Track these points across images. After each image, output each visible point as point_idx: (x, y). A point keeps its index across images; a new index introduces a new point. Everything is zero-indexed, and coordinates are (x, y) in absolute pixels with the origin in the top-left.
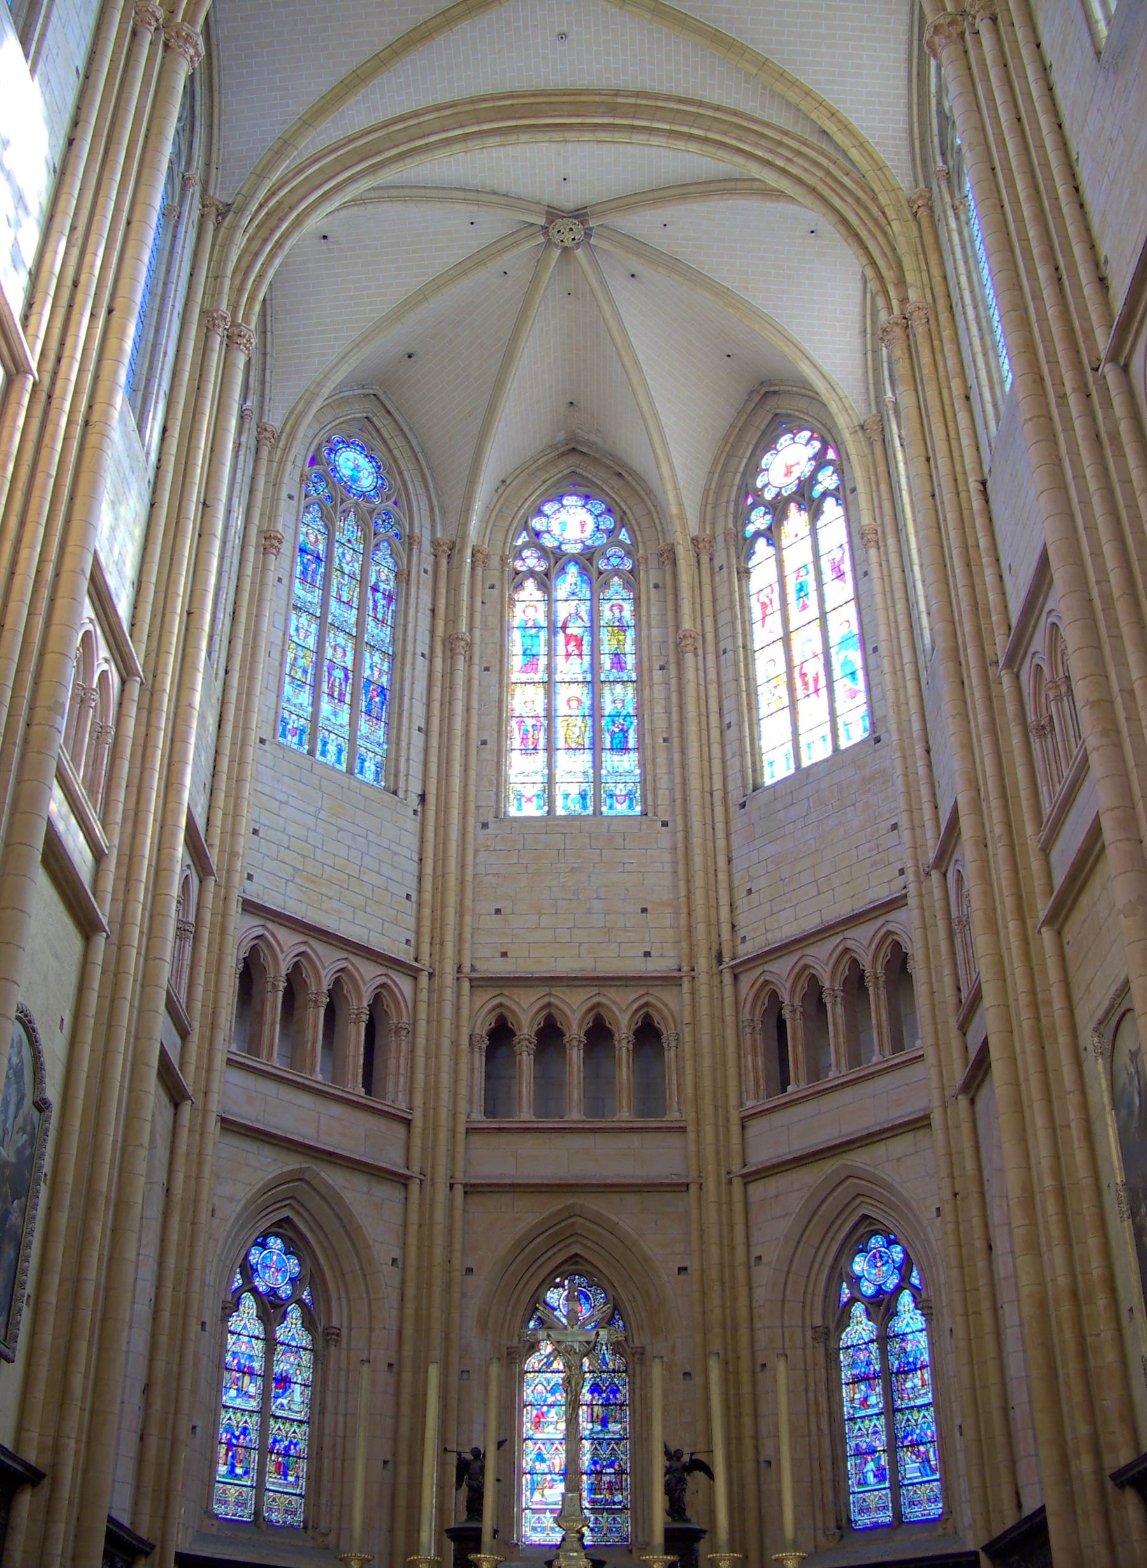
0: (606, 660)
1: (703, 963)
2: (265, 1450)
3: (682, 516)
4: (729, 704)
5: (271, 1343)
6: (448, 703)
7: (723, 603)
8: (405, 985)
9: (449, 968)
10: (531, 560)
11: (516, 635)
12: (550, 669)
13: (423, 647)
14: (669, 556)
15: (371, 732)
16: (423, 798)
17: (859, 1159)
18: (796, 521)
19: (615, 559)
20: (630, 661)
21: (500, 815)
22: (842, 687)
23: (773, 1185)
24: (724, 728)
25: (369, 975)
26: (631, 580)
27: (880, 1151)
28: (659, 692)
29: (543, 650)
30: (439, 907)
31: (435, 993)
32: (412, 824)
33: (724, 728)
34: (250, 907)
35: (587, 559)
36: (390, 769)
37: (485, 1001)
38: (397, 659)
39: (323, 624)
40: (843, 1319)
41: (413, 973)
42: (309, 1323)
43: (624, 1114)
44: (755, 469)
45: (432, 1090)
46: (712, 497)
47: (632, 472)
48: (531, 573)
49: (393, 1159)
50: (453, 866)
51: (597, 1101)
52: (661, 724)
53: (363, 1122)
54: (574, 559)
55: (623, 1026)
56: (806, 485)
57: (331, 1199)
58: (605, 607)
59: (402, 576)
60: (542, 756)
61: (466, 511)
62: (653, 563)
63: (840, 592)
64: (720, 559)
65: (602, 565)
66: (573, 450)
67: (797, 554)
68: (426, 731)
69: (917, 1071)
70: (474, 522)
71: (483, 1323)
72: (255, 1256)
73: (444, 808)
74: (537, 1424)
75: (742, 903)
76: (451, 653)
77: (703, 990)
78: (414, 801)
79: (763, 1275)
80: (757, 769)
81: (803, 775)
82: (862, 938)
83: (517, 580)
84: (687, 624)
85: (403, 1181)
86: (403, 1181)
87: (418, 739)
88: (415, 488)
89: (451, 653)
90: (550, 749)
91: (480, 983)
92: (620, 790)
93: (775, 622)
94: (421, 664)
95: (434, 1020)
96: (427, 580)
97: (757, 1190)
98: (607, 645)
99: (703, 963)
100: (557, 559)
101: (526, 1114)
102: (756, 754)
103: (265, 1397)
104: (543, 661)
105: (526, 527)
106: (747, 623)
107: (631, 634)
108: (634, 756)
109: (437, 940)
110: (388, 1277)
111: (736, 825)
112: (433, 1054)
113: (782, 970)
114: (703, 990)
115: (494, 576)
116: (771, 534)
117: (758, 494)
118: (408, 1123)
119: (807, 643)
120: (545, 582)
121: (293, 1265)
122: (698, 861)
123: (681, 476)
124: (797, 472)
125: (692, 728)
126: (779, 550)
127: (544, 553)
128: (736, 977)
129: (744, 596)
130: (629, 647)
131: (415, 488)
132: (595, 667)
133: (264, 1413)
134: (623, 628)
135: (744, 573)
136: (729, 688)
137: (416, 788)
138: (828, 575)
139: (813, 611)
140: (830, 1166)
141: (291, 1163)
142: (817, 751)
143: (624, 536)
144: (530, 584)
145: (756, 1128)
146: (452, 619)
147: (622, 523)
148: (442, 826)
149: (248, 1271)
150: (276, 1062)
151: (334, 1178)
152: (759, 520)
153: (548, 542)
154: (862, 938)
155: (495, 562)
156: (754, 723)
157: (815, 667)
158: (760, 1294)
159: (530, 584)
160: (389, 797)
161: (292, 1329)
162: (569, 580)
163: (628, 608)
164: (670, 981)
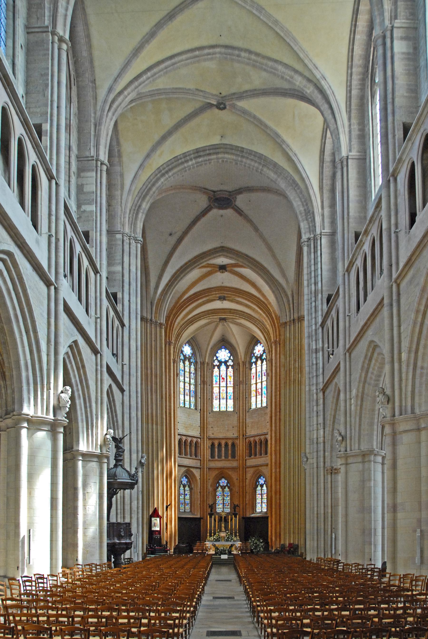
0: (228, 383)
1: (241, 437)
2: (185, 503)
3: (241, 358)
4: (247, 394)
5: (185, 490)
6: (204, 393)
7: (247, 375)
8: (199, 440)
9: (205, 437)
10: (216, 363)
11: (214, 377)
12: (220, 384)
13: (199, 383)
14: (239, 364)
15: (193, 400)
16: (201, 410)
17: (260, 468)
18: (259, 362)
19: (230, 363)
20: (232, 383)
21: (212, 411)
22: (263, 395)
23: (249, 469)
24: (246, 398)
25: (195, 440)
26: (233, 367)
27: (262, 467)
28: (236, 390)
29: (218, 381)
30: (204, 427)
31: (204, 441)
32: (199, 414)
33: (246, 398)
34: (179, 435)
35: (226, 362)
36: (196, 405)
37: (211, 442)
38: (196, 385)
39: (184, 383)
40: (257, 487)
41: (200, 438)
42: (189, 487)
43: (230, 458)
44: (254, 349)
45: (204, 455)
46: (246, 354)
47: (233, 346)
48: (216, 365)
49: (198, 465)
50: (205, 421)
51: (226, 456)
52: (236, 396)
53: (195, 461)
54: (223, 362)
55: (230, 444)
56: (261, 356)
57: (192, 472)
58: (228, 372)
59: (196, 369)
60: (218, 400)
61: (206, 357)
62: (236, 364)
63: (264, 378)
64: (247, 366)
65: (228, 364)
66: (223, 341)
67: (259, 369)
68: (200, 398)
69: (268, 458)
70: (207, 358)
71: (211, 486)
72: (182, 480)
73: (204, 412)
74: (218, 497)
75: (247, 427)
76: (204, 384)
77: (241, 441)
78: (199, 411)
79: (247, 481)
80: (251, 406)
81: (257, 409)
82: (262, 437)
83: (214, 366)
84: (241, 379)
85: (200, 468)
86: (200, 468)
87: (199, 399)
88: (197, 351)
89: (204, 384)
90: (220, 399)
91: (209, 439)
92: (230, 406)
93: (255, 379)
94: (199, 386)
95: (204, 445)
96: (199, 369)
97: (247, 469)
98: (228, 380)
99: (241, 437)
100: (220, 362)
101: (216, 458)
102: (251, 403)
103: (184, 497)
104: (218, 383)
105: (215, 355)
106: (251, 379)
107: (232, 377)
108: (232, 400)
109: (204, 433)
110: (199, 481)
111: (247, 415)
112: (204, 450)
113: (252, 439)
114: (241, 441)
115: (210, 366)
116: (256, 363)
117: (254, 354)
118: (201, 460)
119: (259, 386)
120: (219, 367)
121: (186, 480)
122: (241, 421)
123: (241, 351)
124: (260, 352)
125: (241, 398)
126: (256, 367)
127: (219, 361)
128: (246, 439)
129: (250, 374)
130: (232, 380)
131: (197, 351)
132: (227, 384)
133: (184, 499)
134: (231, 377)
135: (251, 369)
136: (247, 391)
137: (199, 408)
138: (263, 375)
139: (260, 381)
140: (257, 468)
141: (186, 469)
142: (259, 406)
143: (232, 358)
144: (216, 367)
145: (247, 461)
146: (204, 378)
147: (231, 355)
148: (204, 414)
149: (181, 482)
150: (184, 456)
151: (192, 469)
152: (254, 360)
153: (219, 359)
154: (262, 437)
155: (210, 364)
156: (251, 398)
157: (260, 390)
158: (247, 483)
159: (216, 367)
160: (196, 411)
161: (187, 488)
162: (223, 367)
163: (232, 372)
164: (236, 439)
